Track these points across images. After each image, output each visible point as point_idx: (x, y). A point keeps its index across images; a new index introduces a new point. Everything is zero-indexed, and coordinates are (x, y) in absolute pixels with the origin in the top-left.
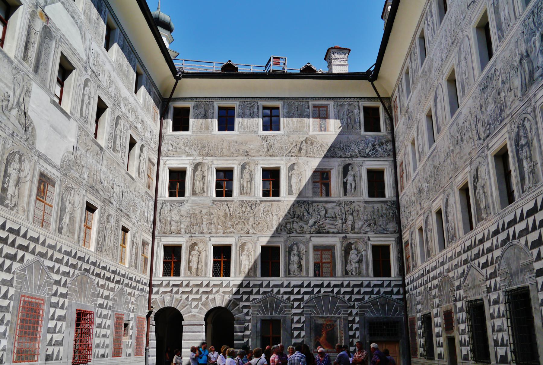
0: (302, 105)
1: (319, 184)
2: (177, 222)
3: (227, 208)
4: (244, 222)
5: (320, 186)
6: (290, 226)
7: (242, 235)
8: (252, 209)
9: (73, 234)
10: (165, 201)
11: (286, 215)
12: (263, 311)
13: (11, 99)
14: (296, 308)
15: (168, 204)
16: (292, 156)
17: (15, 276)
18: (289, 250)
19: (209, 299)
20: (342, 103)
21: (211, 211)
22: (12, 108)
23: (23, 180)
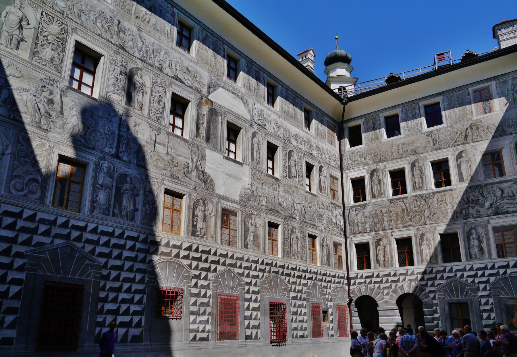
0: (462, 94)
1: (491, 165)
2: (363, 223)
3: (404, 204)
4: (420, 215)
5: (492, 168)
6: (466, 211)
7: (420, 227)
8: (426, 202)
9: (259, 247)
10: (351, 207)
11: (460, 202)
12: (449, 295)
13: (190, 166)
15: (354, 209)
16: (458, 145)
17: (211, 282)
18: (467, 235)
19: (398, 287)
20: (504, 79)
21: (390, 209)
22: (192, 171)
23: (208, 216)
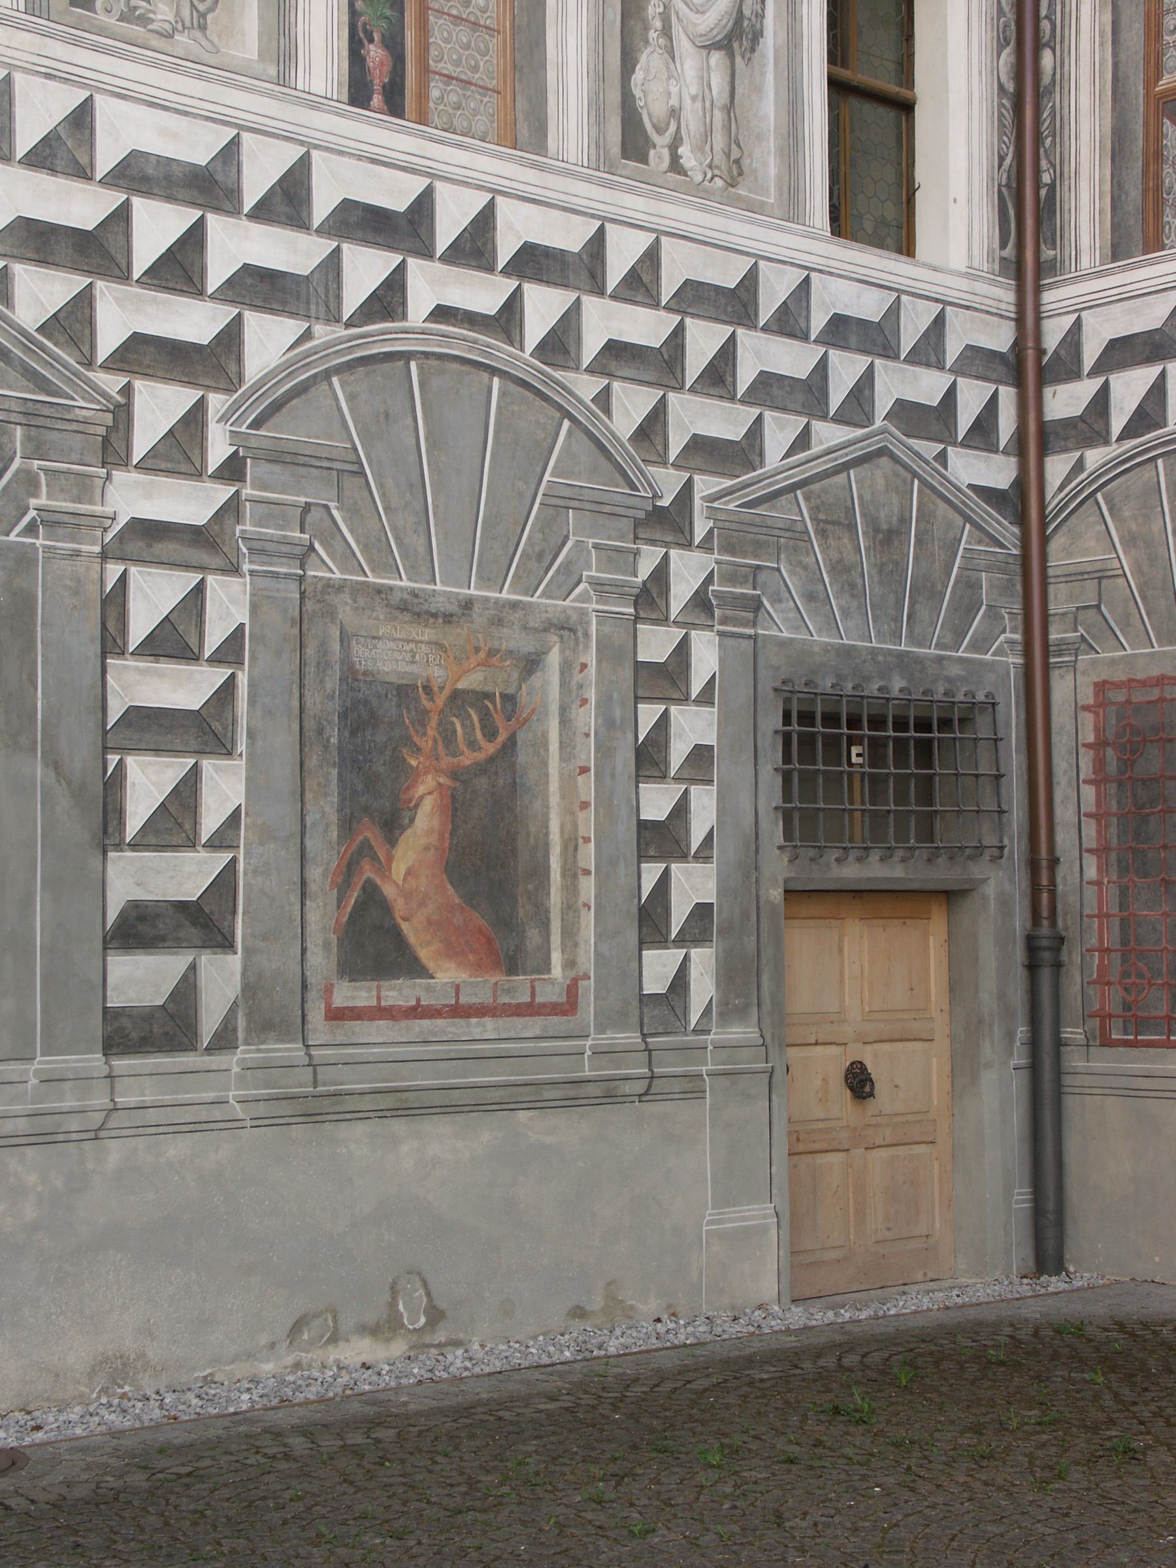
14: (153, 463)
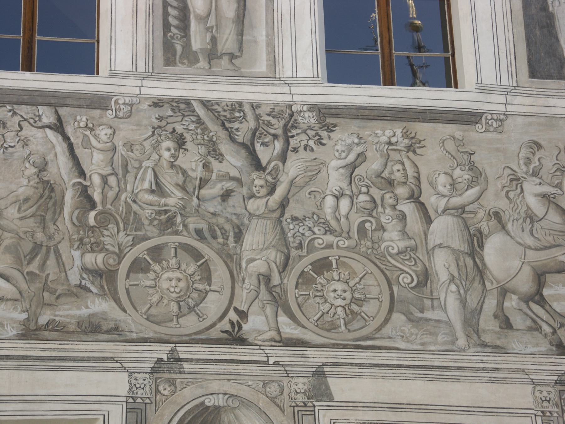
3: (60, 147)
4: (196, 255)
7: (183, 352)
